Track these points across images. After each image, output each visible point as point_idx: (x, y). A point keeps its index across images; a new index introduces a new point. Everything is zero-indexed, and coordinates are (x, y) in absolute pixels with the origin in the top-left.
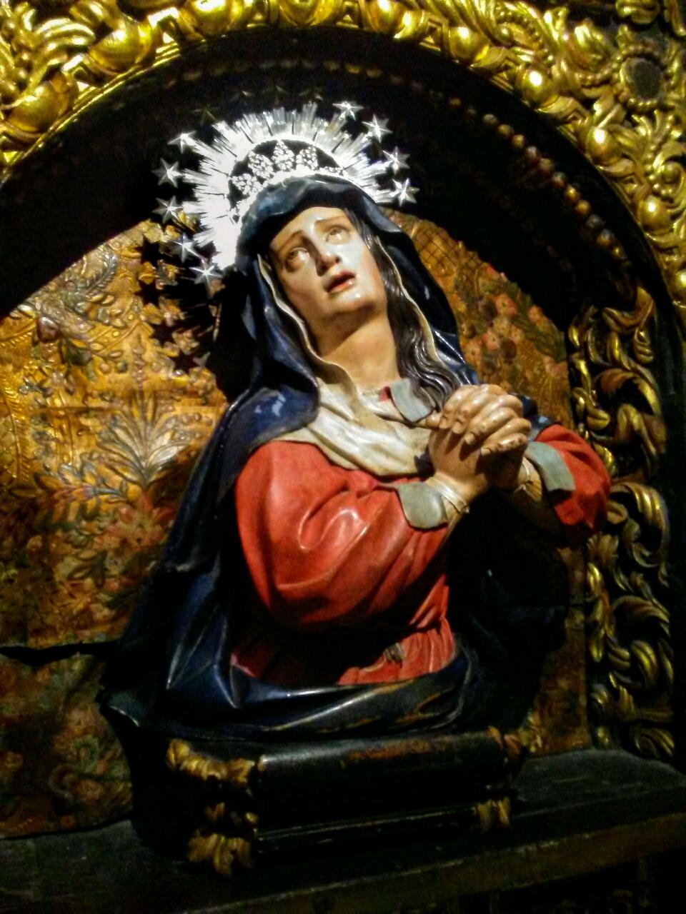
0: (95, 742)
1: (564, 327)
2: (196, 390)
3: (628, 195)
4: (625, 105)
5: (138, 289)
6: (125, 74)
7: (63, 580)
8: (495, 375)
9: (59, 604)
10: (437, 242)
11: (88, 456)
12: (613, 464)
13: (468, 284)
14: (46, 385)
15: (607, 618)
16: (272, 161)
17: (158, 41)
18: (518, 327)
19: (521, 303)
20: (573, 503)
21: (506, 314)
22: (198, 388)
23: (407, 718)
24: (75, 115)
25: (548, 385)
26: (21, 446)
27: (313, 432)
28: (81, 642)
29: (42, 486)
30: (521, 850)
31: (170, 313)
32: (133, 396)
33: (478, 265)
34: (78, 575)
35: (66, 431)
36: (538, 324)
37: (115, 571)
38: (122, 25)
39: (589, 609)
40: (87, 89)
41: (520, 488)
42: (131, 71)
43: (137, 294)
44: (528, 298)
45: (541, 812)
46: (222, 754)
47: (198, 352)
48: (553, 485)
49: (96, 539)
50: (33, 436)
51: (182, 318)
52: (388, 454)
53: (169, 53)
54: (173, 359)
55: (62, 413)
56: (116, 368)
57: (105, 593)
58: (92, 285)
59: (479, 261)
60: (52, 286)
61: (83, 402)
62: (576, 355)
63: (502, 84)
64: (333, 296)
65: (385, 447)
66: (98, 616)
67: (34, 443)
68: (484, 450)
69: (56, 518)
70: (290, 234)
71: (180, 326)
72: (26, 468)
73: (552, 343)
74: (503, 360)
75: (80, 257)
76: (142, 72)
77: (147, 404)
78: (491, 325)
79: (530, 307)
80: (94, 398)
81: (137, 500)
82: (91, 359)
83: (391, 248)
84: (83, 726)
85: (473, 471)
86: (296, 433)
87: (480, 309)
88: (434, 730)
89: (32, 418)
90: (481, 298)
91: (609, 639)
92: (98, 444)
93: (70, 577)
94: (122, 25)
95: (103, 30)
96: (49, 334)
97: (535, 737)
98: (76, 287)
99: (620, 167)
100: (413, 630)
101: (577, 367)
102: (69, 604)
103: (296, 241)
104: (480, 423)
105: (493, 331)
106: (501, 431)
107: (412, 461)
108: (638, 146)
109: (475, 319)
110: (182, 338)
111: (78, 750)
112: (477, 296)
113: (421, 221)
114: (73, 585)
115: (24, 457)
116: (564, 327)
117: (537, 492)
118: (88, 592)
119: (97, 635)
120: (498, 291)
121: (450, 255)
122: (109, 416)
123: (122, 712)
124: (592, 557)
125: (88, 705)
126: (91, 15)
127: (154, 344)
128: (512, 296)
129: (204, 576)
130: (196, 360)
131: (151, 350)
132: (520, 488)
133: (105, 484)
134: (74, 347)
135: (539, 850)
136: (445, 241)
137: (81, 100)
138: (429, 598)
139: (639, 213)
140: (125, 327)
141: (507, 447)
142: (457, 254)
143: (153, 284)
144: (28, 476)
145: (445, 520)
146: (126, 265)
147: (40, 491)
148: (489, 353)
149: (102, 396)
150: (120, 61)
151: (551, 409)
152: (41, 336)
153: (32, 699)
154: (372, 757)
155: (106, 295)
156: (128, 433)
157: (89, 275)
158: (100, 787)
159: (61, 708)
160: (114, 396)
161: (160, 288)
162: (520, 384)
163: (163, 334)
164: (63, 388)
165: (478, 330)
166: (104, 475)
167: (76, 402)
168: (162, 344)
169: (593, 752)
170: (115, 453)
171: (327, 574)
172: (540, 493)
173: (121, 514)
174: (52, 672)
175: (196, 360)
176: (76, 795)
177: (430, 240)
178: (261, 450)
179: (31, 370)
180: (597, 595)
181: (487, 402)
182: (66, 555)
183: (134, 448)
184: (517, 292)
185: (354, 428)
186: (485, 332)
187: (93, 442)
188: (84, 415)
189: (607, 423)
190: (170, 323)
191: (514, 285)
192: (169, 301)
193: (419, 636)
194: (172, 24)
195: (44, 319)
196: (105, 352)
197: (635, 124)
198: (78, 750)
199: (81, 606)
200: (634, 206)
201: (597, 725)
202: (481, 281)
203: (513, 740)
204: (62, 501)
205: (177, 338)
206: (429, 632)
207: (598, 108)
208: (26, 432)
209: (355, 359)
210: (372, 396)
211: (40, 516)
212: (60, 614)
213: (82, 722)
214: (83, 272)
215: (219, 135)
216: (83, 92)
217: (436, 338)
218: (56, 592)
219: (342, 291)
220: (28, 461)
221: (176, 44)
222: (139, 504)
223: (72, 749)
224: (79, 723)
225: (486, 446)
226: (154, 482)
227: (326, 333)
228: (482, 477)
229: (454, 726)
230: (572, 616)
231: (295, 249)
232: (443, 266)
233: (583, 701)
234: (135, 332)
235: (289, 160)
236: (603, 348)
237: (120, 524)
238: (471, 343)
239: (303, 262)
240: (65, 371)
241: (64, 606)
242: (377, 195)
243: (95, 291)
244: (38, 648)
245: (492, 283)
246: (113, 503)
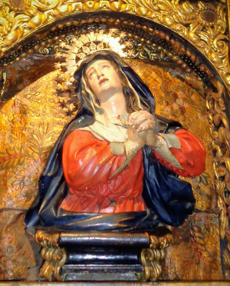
10: (153, 73)
13: (166, 87)
18: (186, 102)
21: (182, 98)
78: (175, 101)
82: (29, 112)
87: (171, 96)
109: (168, 99)
128: (184, 92)
142: (161, 77)
177: (151, 73)
196: (34, 110)
202: (171, 87)
238: (167, 108)
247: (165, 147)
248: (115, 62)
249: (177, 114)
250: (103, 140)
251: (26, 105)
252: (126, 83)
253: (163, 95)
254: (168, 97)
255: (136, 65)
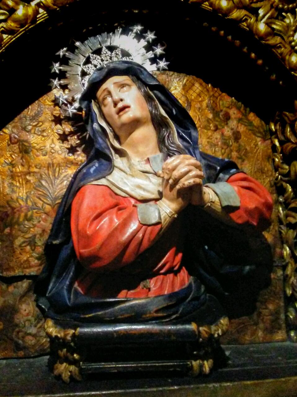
0: (33, 319)
1: (268, 123)
2: (77, 162)
3: (279, 54)
4: (277, 8)
5: (53, 118)
6: (24, 28)
7: (17, 247)
8: (229, 149)
9: (16, 258)
10: (197, 85)
11: (29, 193)
12: (291, 192)
14: (14, 162)
15: (293, 273)
16: (101, 57)
17: (36, 12)
18: (242, 124)
19: (244, 112)
20: (241, 212)
21: (235, 118)
22: (78, 161)
23: (148, 315)
24: (4, 48)
25: (259, 153)
26: (2, 189)
27: (108, 180)
28: (25, 274)
29: (10, 206)
30: (211, 385)
31: (68, 128)
32: (50, 166)
33: (220, 95)
34: (23, 245)
35: (21, 182)
36: (254, 122)
37: (39, 244)
38: (21, 7)
39: (284, 268)
40: (7, 37)
41: (207, 205)
42: (26, 26)
43: (52, 121)
44: (248, 109)
45: (237, 369)
46: (63, 325)
47: (79, 145)
48: (225, 204)
49: (31, 229)
50: (7, 184)
51: (72, 130)
52: (144, 190)
53: (43, 16)
54: (67, 148)
55: (19, 174)
56: (42, 154)
57: (36, 253)
58: (33, 118)
59: (220, 93)
60: (16, 119)
61: (28, 169)
62: (273, 137)
63: (206, 8)
64: (120, 117)
65: (143, 186)
66: (33, 263)
67: (8, 188)
68: (178, 187)
69: (15, 220)
70: (103, 90)
71: (72, 133)
72: (4, 199)
73: (262, 130)
74: (233, 141)
75: (28, 106)
76: (32, 26)
77: (55, 170)
78: (227, 124)
79: (249, 113)
80: (33, 167)
81: (49, 212)
83: (155, 92)
84: (27, 311)
85: (176, 197)
86: (99, 181)
87: (221, 116)
88: (163, 322)
89: (7, 177)
90: (221, 111)
91: (294, 285)
92: (34, 187)
93: (20, 246)
94: (21, 7)
95: (12, 11)
96: (14, 141)
97: (218, 330)
98: (26, 120)
99: (272, 41)
100: (157, 273)
101: (274, 143)
102: (20, 257)
103: (106, 93)
104: (176, 174)
105: (228, 127)
106: (186, 177)
107: (157, 193)
108: (284, 29)
109: (217, 121)
110: (73, 139)
111: (25, 322)
112: (219, 110)
113: (188, 76)
114: (22, 249)
115: (3, 194)
116: (268, 123)
117: (218, 208)
118: (28, 252)
119: (33, 271)
120: (231, 107)
121: (204, 91)
122: (39, 175)
123: (43, 307)
124: (285, 242)
125: (31, 303)
126: (8, 6)
127: (60, 143)
128: (239, 109)
129: (66, 246)
130: (78, 149)
131: (57, 145)
132: (207, 205)
133: (36, 205)
134: (25, 146)
135: (220, 386)
136: (201, 84)
137: (5, 42)
138: (165, 259)
139: (287, 63)
140: (48, 136)
141: (187, 185)
142: (208, 90)
143: (59, 116)
144: (4, 202)
145: (160, 221)
146: (48, 108)
147: (9, 208)
148: (226, 138)
149: (36, 167)
150: (22, 23)
151: (261, 165)
152: (11, 141)
153: (6, 299)
154: (129, 332)
155: (39, 122)
156: (47, 182)
157: (32, 114)
158: (34, 339)
159: (17, 303)
160: (41, 166)
161: (62, 118)
162: (243, 152)
163: (63, 138)
164: (20, 164)
165: (219, 127)
166: (35, 201)
167: (25, 170)
168: (63, 143)
169: (288, 343)
170: (40, 191)
171: (97, 245)
172: (220, 207)
173: (42, 218)
174: (15, 287)
175: (78, 149)
176: (24, 341)
177: (193, 85)
178: (82, 189)
179: (7, 156)
180: (287, 261)
181: (179, 163)
182: (19, 236)
183: (49, 189)
184: (241, 106)
185: (130, 178)
186: (223, 127)
187: (32, 187)
188: (29, 175)
189: (287, 171)
190: (67, 133)
191: (240, 103)
192: (66, 123)
193: (162, 276)
194: (42, 4)
195: (13, 135)
196: (38, 147)
197: (284, 17)
198: (25, 322)
199: (25, 258)
200: (284, 59)
201: (291, 330)
202: (221, 102)
203: (205, 331)
204: (17, 213)
205: (70, 139)
206: (168, 275)
207: (261, 12)
208: (5, 183)
209: (134, 146)
210: (142, 162)
211: (9, 219)
212: (16, 262)
213: (27, 310)
214: (29, 113)
215: (77, 48)
216: (5, 39)
217: (178, 133)
218: (14, 252)
219: (123, 114)
220: (4, 196)
221: (45, 12)
222: (51, 214)
223: (22, 321)
224: (25, 310)
225: (179, 185)
226: (57, 204)
227: (121, 134)
228: (180, 199)
229: (174, 321)
230: (275, 272)
231: (106, 96)
232: (200, 97)
233: (282, 316)
234: (51, 138)
235: (108, 56)
236: (283, 132)
237: (42, 222)
238: (215, 133)
239: (109, 102)
240: (21, 156)
241: (17, 258)
242: (151, 68)
243: (34, 121)
244: (7, 276)
245: (228, 103)
246: (38, 213)
247: (217, 204)
248: (139, 79)
249: (229, 142)
250: (127, 196)
251: (26, 141)
252: (156, 108)
253: (211, 116)
254: (217, 119)
255: (173, 75)
